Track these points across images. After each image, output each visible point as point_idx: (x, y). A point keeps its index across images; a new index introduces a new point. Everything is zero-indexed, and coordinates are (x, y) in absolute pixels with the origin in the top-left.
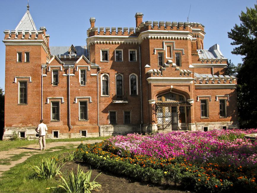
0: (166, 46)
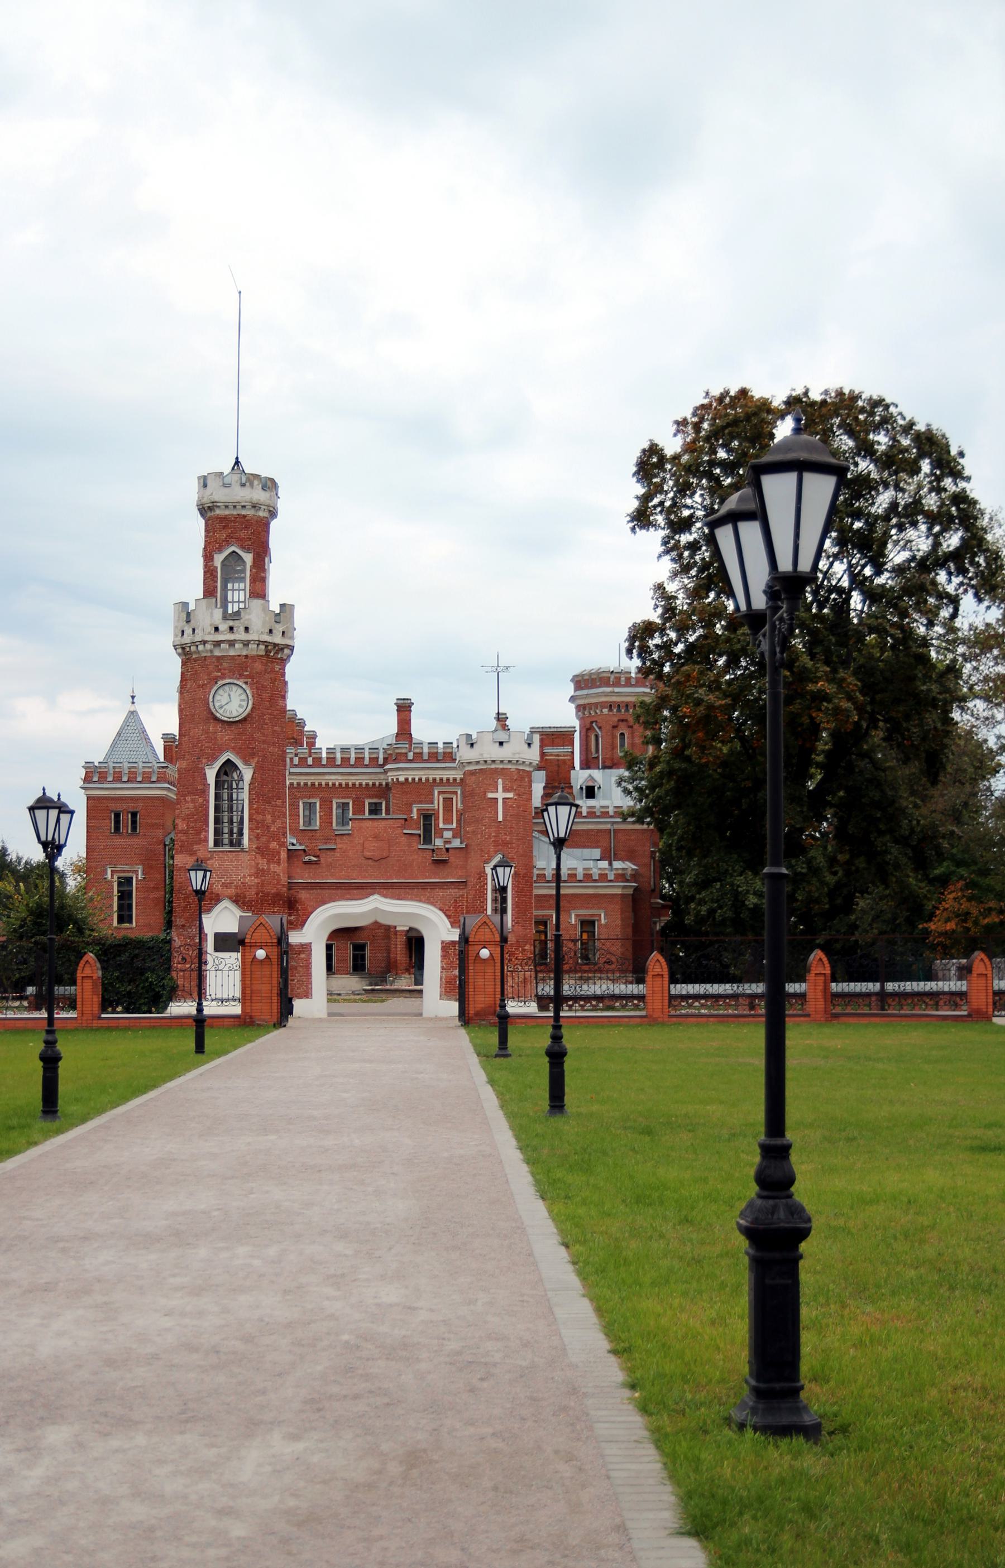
0: (441, 800)
